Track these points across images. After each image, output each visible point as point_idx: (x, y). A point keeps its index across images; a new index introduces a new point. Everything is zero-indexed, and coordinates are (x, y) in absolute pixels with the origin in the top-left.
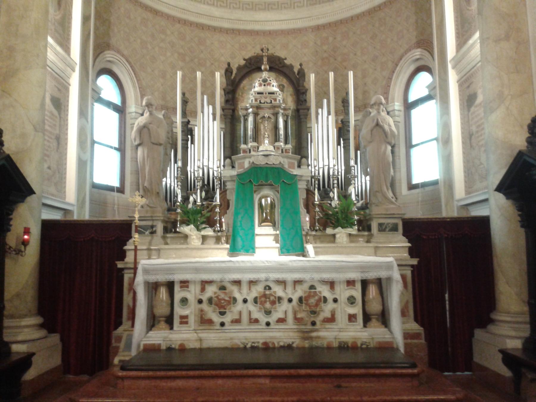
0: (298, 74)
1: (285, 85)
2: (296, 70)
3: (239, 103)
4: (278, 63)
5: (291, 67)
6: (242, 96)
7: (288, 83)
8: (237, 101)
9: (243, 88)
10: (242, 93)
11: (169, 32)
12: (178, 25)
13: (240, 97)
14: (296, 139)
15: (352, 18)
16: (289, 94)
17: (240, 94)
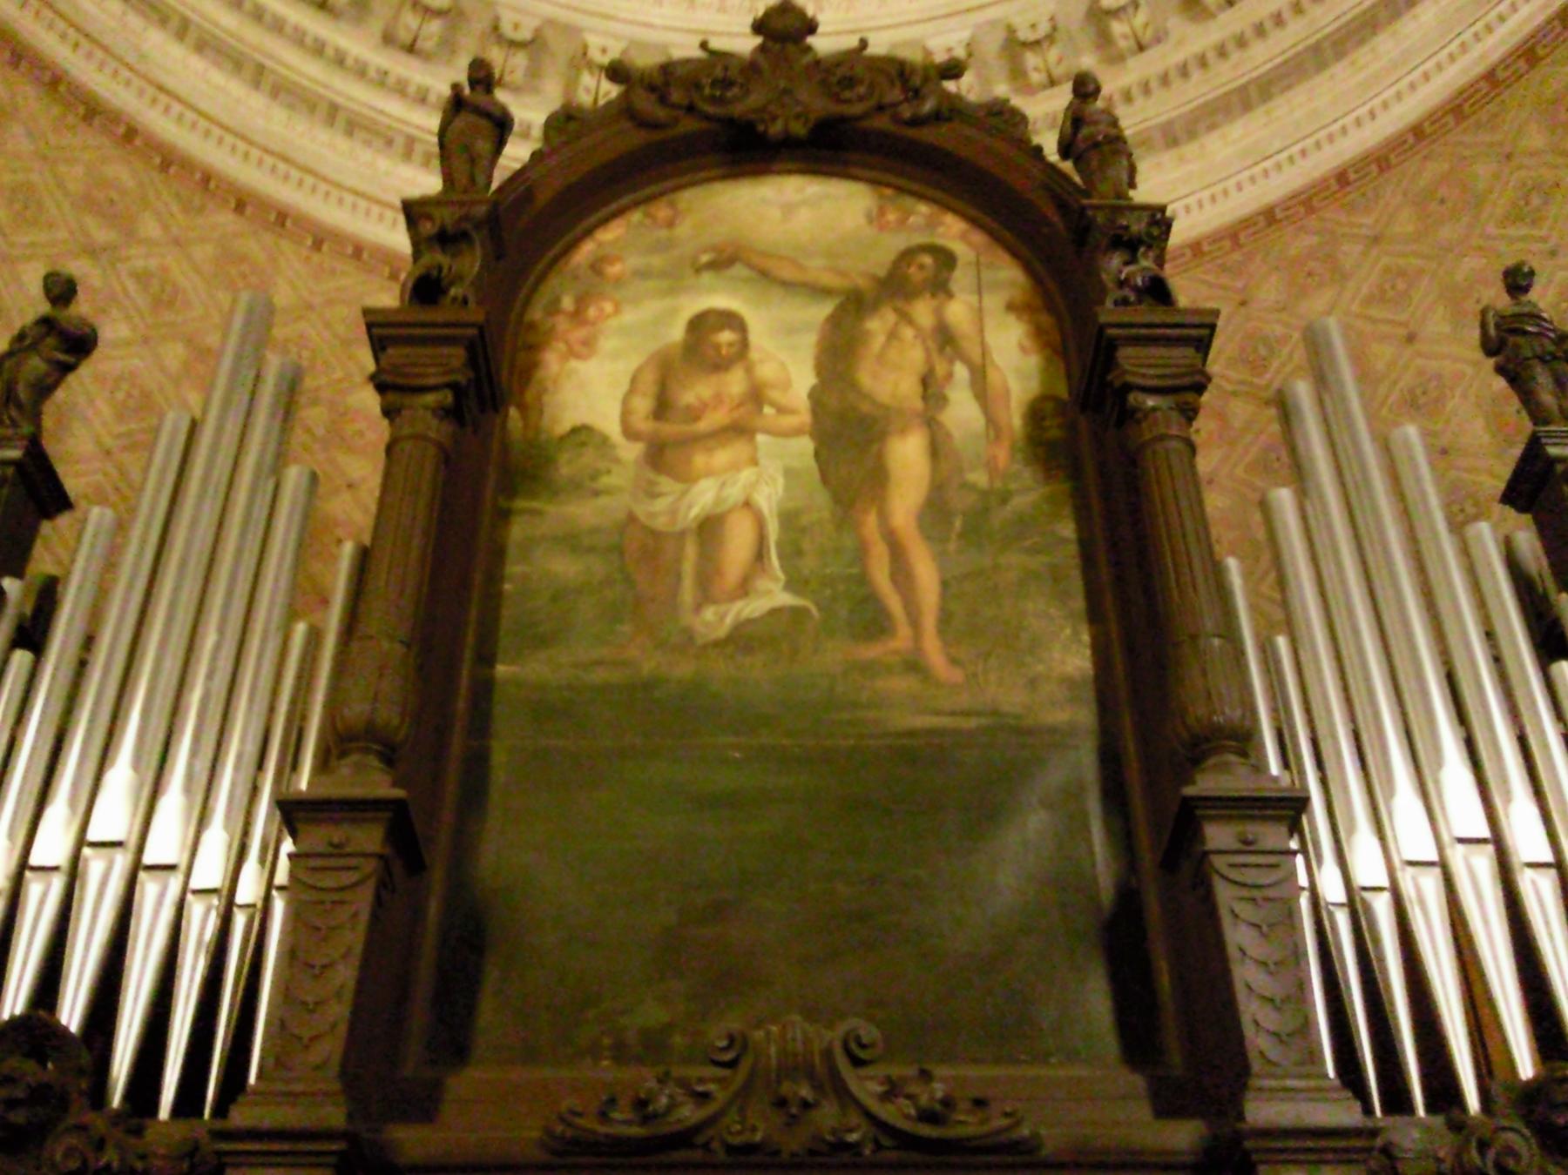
0: (1065, 150)
1: (958, 248)
2: (1049, 143)
3: (551, 360)
4: (895, 94)
5: (1003, 120)
6: (578, 315)
7: (979, 238)
8: (534, 348)
9: (596, 267)
10: (582, 302)
11: (150, 227)
12: (225, 219)
13: (562, 324)
14: (1095, 615)
15: (1342, 178)
16: (994, 302)
17: (567, 303)
